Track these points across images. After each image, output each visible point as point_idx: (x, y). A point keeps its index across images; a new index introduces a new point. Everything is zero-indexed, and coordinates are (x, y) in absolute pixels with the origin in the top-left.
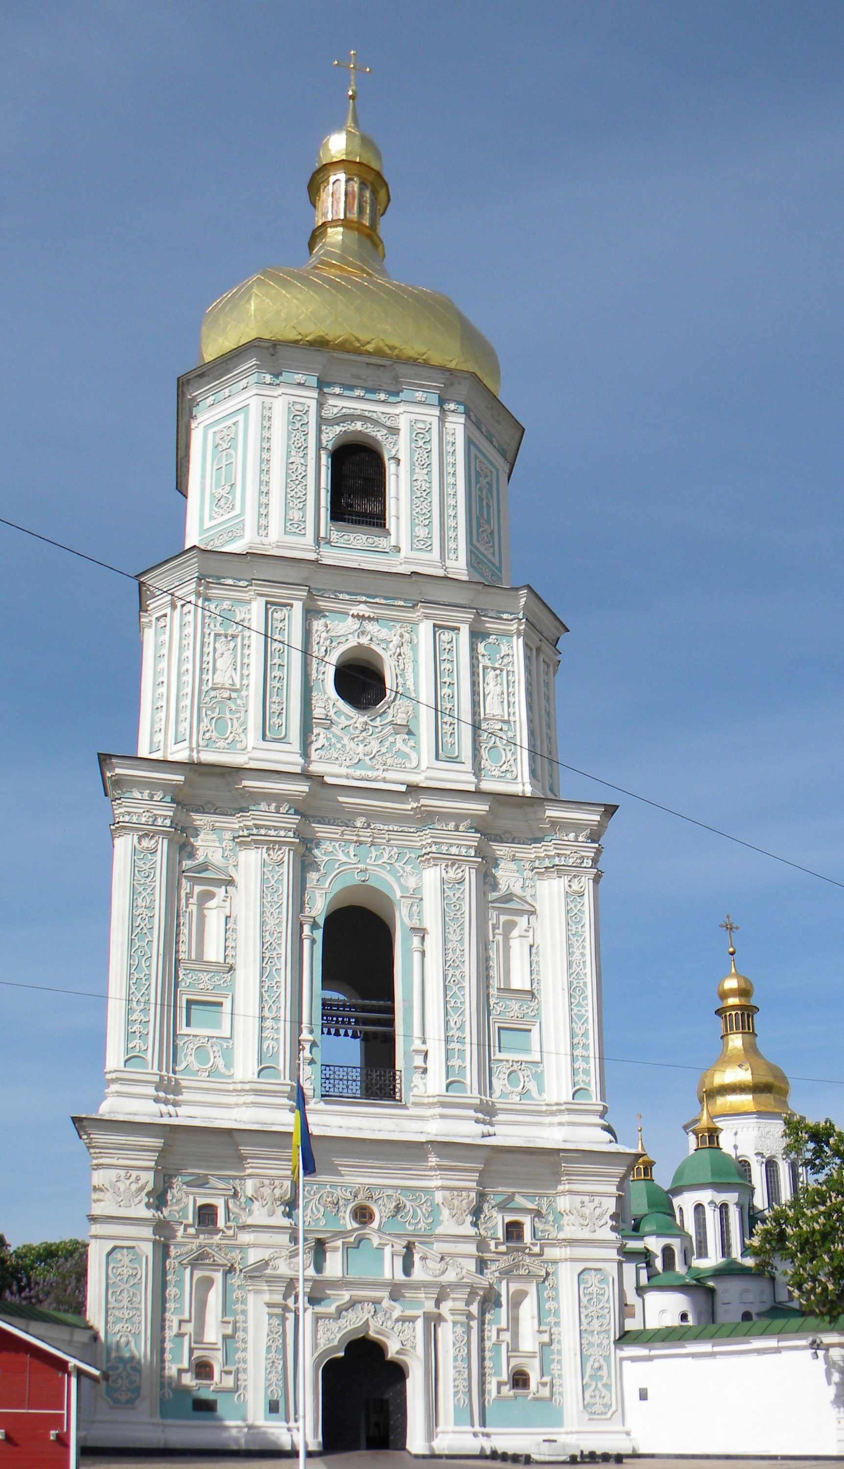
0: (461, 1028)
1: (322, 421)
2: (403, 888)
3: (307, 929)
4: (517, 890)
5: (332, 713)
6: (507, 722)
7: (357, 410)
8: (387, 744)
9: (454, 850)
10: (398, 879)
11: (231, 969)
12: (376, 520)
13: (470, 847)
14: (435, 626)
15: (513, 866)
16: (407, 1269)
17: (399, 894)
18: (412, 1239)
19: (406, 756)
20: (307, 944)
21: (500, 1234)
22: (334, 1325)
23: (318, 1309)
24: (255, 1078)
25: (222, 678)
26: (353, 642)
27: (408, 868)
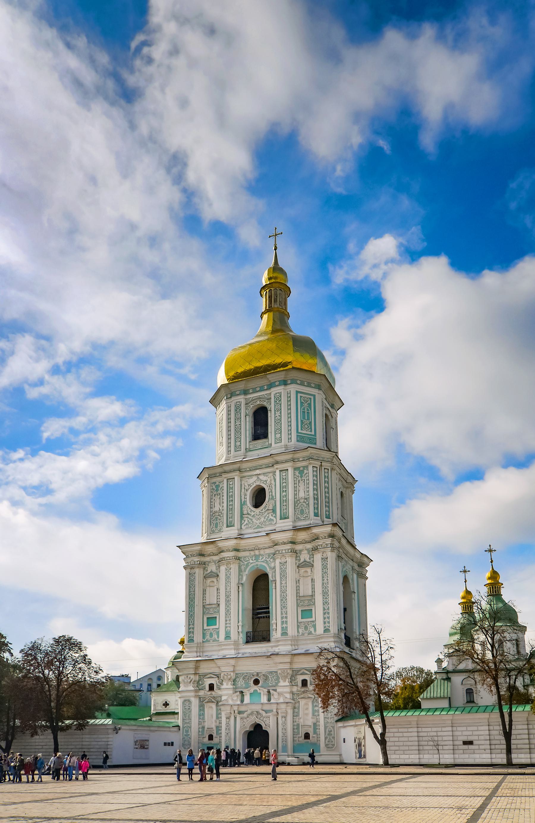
0: (286, 614)
1: (246, 404)
2: (270, 568)
3: (240, 588)
4: (308, 560)
5: (249, 512)
6: (306, 499)
7: (257, 398)
8: (266, 518)
9: (284, 551)
10: (268, 565)
11: (219, 605)
12: (265, 436)
13: (288, 550)
14: (280, 471)
15: (307, 552)
16: (269, 700)
17: (268, 569)
18: (269, 688)
19: (273, 520)
20: (240, 593)
21: (300, 684)
22: (245, 720)
23: (242, 715)
24: (223, 640)
25: (216, 509)
26: (254, 485)
27: (272, 560)
